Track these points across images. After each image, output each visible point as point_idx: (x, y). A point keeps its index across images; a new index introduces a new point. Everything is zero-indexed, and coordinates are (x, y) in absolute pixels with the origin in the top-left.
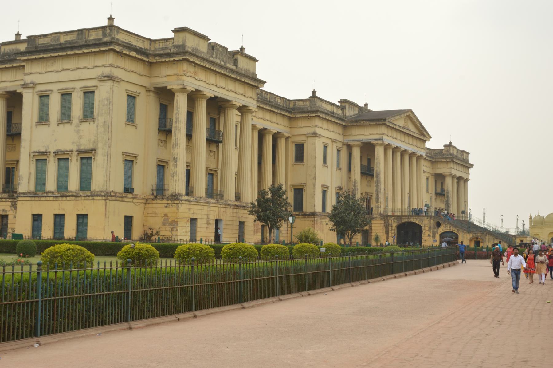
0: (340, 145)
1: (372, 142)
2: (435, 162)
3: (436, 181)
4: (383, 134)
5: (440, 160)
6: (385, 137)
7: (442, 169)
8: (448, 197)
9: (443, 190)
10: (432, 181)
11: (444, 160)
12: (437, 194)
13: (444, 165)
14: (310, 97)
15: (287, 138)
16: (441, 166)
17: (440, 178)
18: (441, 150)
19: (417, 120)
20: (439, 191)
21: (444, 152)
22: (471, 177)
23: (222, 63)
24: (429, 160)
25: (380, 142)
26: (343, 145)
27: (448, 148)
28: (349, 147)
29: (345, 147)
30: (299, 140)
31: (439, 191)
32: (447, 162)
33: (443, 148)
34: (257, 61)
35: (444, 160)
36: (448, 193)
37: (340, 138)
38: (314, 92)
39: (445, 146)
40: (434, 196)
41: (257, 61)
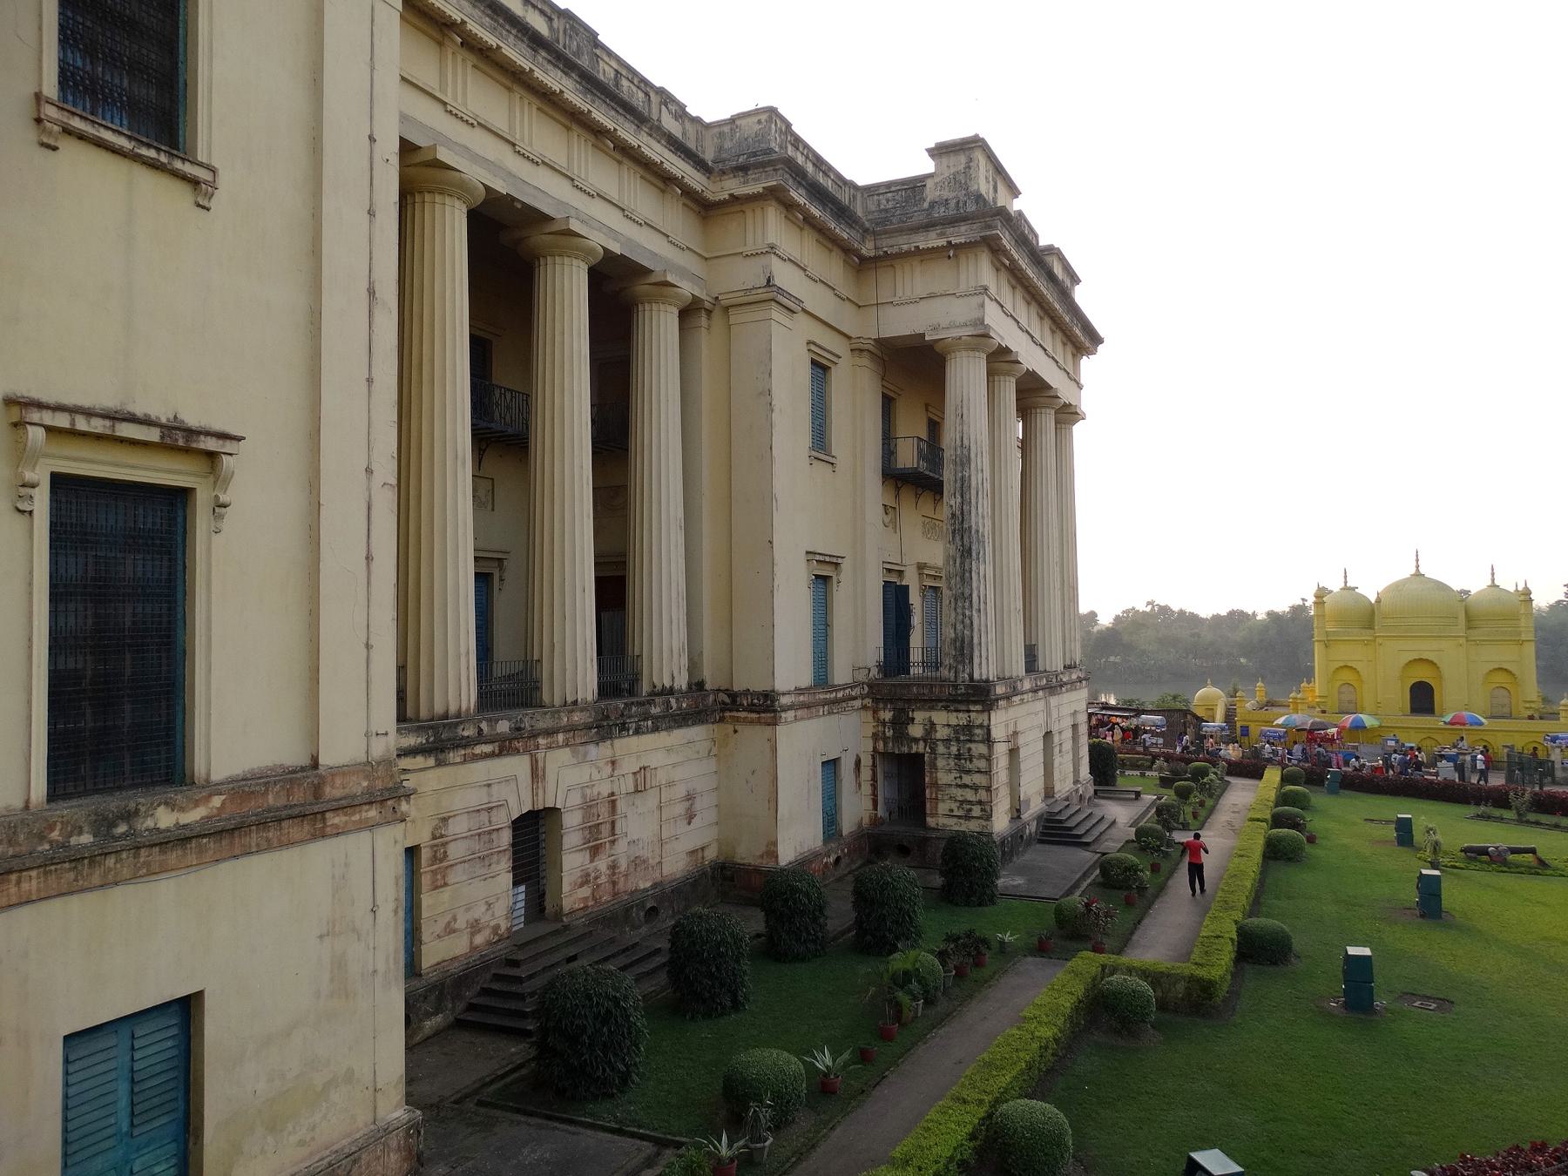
2: (876, 259)
3: (888, 404)
5: (904, 243)
7: (923, 305)
8: (964, 486)
9: (932, 446)
10: (856, 395)
11: (933, 240)
12: (897, 479)
13: (935, 277)
16: (915, 280)
17: (913, 368)
18: (913, 186)
19: (819, 162)
20: (907, 457)
21: (931, 193)
22: (1087, 401)
24: (810, 222)
27: (963, 159)
31: (907, 457)
32: (953, 252)
33: (927, 166)
35: (933, 240)
36: (964, 461)
39: (940, 151)
40: (874, 491)
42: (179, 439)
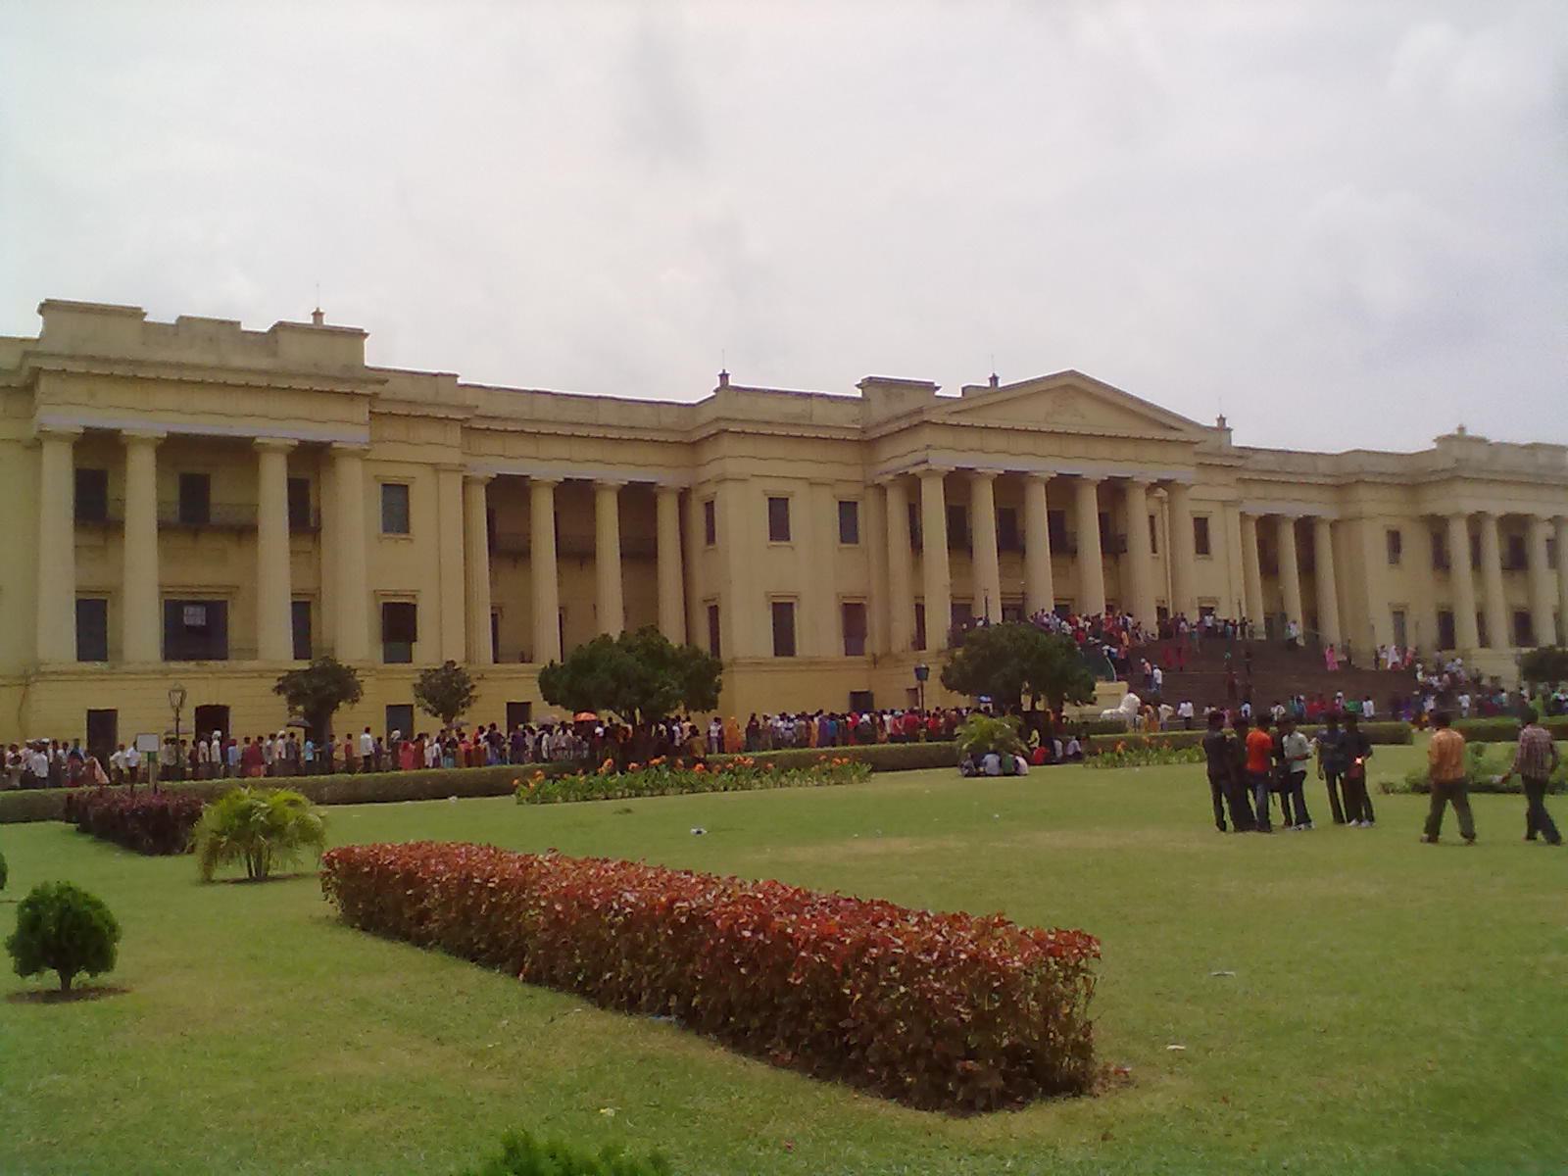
0: (849, 493)
1: (911, 471)
4: (928, 447)
6: (932, 455)
14: (716, 391)
15: (683, 497)
23: (210, 359)
25: (923, 467)
26: (866, 487)
28: (882, 490)
29: (871, 491)
30: (707, 491)
34: (366, 335)
37: (856, 473)
38: (724, 376)
41: (366, 335)
42: (1210, 600)
